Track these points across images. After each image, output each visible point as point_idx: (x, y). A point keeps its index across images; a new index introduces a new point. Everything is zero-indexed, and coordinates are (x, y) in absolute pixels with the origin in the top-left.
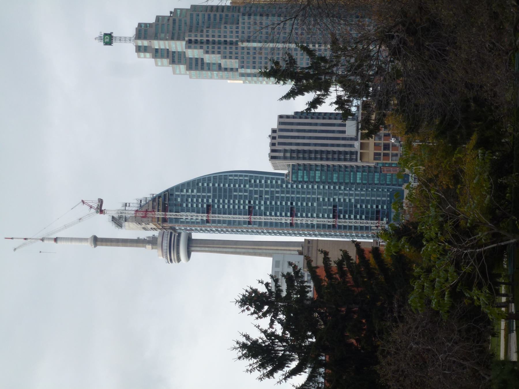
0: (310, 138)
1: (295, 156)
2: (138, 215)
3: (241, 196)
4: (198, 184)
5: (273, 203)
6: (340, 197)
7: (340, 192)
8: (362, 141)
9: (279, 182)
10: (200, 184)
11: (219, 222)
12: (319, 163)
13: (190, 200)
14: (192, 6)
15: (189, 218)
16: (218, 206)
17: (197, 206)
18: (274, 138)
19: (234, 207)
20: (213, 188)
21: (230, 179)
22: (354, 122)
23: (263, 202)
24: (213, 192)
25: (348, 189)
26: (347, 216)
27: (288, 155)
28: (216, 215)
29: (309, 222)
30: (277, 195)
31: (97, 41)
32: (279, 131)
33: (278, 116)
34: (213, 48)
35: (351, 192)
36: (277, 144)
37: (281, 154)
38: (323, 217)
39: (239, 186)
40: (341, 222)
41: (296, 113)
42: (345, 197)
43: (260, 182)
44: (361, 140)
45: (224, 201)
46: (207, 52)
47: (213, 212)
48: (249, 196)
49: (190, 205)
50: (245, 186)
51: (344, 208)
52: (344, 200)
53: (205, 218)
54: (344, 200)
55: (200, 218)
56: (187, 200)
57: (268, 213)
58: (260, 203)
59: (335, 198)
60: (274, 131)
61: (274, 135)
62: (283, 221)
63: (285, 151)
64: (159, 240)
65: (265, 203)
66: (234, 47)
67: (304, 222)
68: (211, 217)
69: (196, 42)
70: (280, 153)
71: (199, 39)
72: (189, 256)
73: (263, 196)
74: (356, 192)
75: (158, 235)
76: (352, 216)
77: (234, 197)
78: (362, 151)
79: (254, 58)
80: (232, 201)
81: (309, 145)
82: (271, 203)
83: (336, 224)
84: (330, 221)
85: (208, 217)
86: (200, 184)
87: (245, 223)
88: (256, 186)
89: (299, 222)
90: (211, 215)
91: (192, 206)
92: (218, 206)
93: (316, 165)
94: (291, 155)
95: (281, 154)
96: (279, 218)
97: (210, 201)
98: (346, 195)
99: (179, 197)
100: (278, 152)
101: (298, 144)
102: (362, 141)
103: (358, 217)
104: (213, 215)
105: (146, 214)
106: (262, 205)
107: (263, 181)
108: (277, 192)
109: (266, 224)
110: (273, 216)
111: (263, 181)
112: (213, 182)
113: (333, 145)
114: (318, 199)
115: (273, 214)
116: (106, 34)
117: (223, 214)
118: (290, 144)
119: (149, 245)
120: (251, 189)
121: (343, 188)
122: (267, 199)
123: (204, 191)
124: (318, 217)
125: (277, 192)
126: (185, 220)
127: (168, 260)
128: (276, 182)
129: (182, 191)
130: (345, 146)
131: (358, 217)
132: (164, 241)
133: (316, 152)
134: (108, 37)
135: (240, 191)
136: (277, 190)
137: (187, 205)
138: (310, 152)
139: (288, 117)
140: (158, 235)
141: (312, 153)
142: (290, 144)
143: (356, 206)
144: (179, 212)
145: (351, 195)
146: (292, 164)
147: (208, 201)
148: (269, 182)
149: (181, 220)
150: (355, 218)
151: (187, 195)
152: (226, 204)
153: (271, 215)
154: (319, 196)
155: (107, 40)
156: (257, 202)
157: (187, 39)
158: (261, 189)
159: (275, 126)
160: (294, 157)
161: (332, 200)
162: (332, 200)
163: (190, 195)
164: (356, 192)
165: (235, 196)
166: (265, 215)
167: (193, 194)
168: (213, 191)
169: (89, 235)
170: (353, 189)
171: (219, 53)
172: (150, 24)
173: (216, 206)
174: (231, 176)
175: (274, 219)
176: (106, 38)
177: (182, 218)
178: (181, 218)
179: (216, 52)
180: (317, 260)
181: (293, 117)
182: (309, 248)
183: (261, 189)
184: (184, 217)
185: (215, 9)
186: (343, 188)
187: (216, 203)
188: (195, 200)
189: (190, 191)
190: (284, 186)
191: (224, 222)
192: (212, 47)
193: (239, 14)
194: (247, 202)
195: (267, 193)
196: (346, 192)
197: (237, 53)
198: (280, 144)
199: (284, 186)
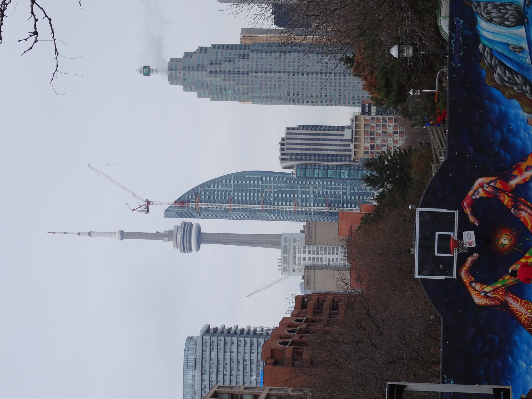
1: (299, 158)
2: (176, 205)
3: (255, 190)
4: (222, 181)
5: (280, 195)
6: (331, 190)
7: (331, 186)
8: (356, 143)
9: (285, 179)
10: (224, 181)
11: (239, 210)
12: (317, 163)
13: (216, 193)
14: (212, 44)
15: (215, 207)
16: (238, 198)
17: (221, 198)
18: (283, 145)
19: (250, 199)
20: (233, 184)
22: (350, 131)
23: (272, 195)
25: (337, 184)
26: (336, 205)
27: (294, 157)
28: (236, 205)
29: (308, 210)
30: (283, 189)
31: (138, 73)
32: (287, 140)
33: (286, 128)
34: (229, 77)
35: (339, 187)
36: (285, 149)
37: (289, 157)
38: (318, 206)
39: (254, 182)
40: (333, 210)
41: (299, 126)
42: (335, 191)
43: (270, 179)
44: (355, 142)
45: (242, 194)
46: (225, 80)
47: (233, 203)
48: (262, 190)
50: (258, 183)
51: (334, 199)
52: (334, 193)
53: (227, 207)
54: (334, 193)
55: (223, 207)
56: (214, 194)
57: (276, 203)
58: (269, 195)
59: (327, 192)
60: (283, 140)
61: (283, 142)
62: (288, 209)
63: (292, 154)
64: (175, 234)
65: (274, 195)
66: (245, 76)
67: (304, 210)
68: (232, 206)
69: (216, 72)
70: (288, 156)
71: (218, 70)
72: (198, 247)
73: (272, 190)
74: (343, 187)
75: (173, 229)
76: (340, 205)
77: (250, 191)
78: (355, 150)
79: (261, 84)
80: (248, 194)
81: (309, 149)
82: (278, 195)
83: (328, 211)
84: (323, 208)
85: (230, 206)
86: (224, 181)
87: (258, 210)
88: (267, 182)
89: (300, 210)
90: (232, 205)
91: (217, 198)
92: (238, 198)
93: (315, 165)
94: (296, 157)
95: (289, 157)
96: (285, 207)
97: (231, 194)
98: (335, 189)
99: (207, 191)
101: (301, 149)
102: (356, 143)
103: (345, 205)
104: (234, 205)
105: (183, 205)
106: (271, 197)
107: (272, 179)
108: (283, 187)
109: (274, 211)
110: (280, 205)
111: (272, 179)
112: (233, 180)
113: (327, 150)
114: (314, 192)
115: (280, 203)
116: (145, 67)
117: (241, 204)
118: (296, 149)
119: (166, 238)
120: (263, 184)
121: (333, 183)
122: (275, 192)
123: (226, 186)
124: (314, 206)
125: (283, 187)
126: (212, 209)
127: (181, 250)
128: (282, 179)
129: (209, 186)
130: (336, 150)
131: (345, 205)
132: (178, 235)
133: (315, 155)
134: (147, 69)
135: (255, 186)
136: (283, 185)
137: (213, 198)
138: (311, 155)
139: (293, 129)
140: (173, 229)
141: (312, 156)
142: (296, 149)
143: (343, 197)
144: (207, 203)
145: (339, 189)
146: (297, 165)
147: (229, 194)
148: (277, 179)
149: (209, 209)
150: (343, 206)
151: (214, 190)
152: (244, 196)
153: (278, 205)
154: (315, 190)
155: (146, 72)
156: (268, 195)
157: (209, 70)
158: (270, 185)
159: (284, 136)
160: (298, 159)
161: (325, 193)
162: (325, 193)
163: (215, 190)
164: (343, 187)
165: (251, 191)
166: (274, 204)
167: (218, 189)
168: (233, 186)
169: (117, 230)
170: (341, 184)
171: (234, 80)
172: (179, 59)
174: (247, 174)
175: (280, 208)
176: (147, 70)
177: (210, 208)
178: (208, 207)
179: (231, 80)
180: (315, 237)
181: (298, 129)
182: (309, 227)
183: (270, 185)
184: (212, 207)
185: (230, 47)
186: (333, 183)
188: (220, 193)
189: (216, 186)
190: (288, 182)
191: (242, 210)
192: (229, 76)
193: (249, 50)
194: (260, 195)
195: (274, 187)
196: (335, 187)
197: (248, 80)
198: (287, 149)
199: (288, 182)
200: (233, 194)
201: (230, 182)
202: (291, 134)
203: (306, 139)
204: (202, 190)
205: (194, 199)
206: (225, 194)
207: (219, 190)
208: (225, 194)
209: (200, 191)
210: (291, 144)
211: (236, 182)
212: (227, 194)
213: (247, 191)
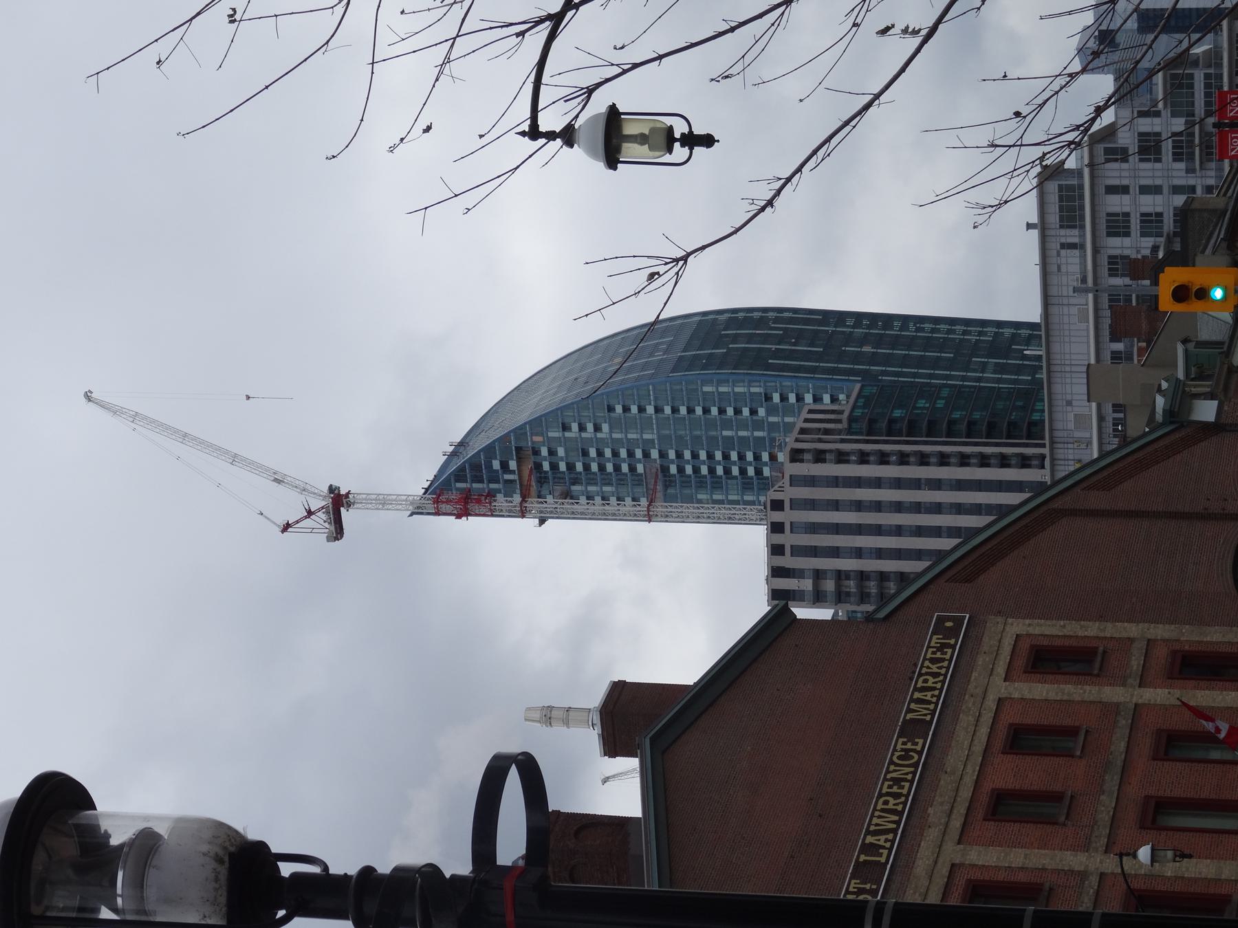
0: (898, 531)
1: (853, 590)
4: (611, 409)
10: (619, 409)
13: (593, 453)
20: (657, 419)
21: (705, 393)
24: (658, 432)
49: (594, 467)
50: (753, 412)
56: (585, 453)
63: (818, 575)
97: (655, 454)
100: (794, 577)
101: (858, 553)
118: (835, 552)
120: (771, 419)
129: (566, 428)
137: (587, 467)
142: (835, 552)
147: (646, 455)
160: (848, 594)
165: (729, 443)
167: (599, 435)
173: (673, 469)
174: (704, 383)
187: (672, 462)
189: (590, 427)
194: (765, 457)
198: (798, 551)
200: (663, 455)
201: (641, 410)
202: (811, 481)
203: (878, 506)
204: (538, 439)
205: (513, 472)
206: (631, 454)
207: (602, 439)
208: (631, 454)
209: (533, 442)
210: (813, 528)
211: (668, 410)
212: (639, 454)
213: (713, 441)
